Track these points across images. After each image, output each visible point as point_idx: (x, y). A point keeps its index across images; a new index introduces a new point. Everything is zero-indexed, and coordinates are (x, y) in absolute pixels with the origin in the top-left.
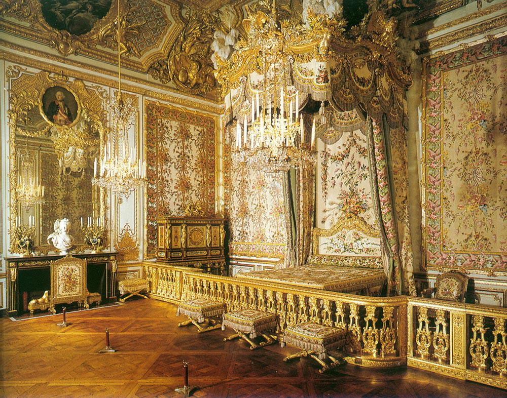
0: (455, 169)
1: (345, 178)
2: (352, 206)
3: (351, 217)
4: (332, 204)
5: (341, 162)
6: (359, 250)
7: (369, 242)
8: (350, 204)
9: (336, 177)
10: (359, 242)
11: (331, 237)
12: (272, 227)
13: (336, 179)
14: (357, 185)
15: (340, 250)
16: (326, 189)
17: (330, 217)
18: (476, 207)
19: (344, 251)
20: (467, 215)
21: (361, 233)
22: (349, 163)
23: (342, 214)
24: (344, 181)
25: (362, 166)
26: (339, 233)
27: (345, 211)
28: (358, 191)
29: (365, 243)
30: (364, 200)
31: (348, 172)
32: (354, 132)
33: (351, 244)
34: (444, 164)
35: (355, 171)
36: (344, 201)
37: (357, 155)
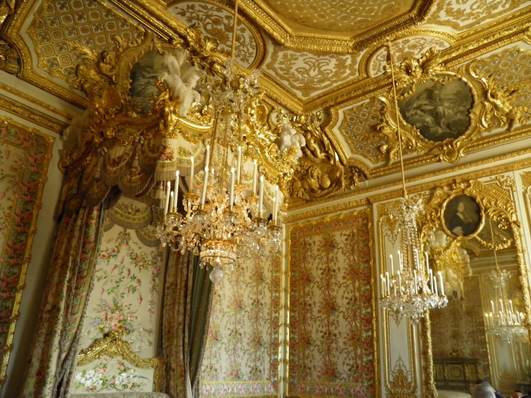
1: (109, 283)
5: (106, 261)
10: (124, 375)
13: (95, 282)
14: (123, 297)
22: (116, 266)
23: (97, 334)
24: (106, 288)
25: (132, 275)
26: (97, 361)
27: (102, 330)
28: (124, 306)
29: (131, 376)
30: (129, 319)
32: (128, 231)
35: (123, 278)
36: (102, 315)
37: (128, 260)
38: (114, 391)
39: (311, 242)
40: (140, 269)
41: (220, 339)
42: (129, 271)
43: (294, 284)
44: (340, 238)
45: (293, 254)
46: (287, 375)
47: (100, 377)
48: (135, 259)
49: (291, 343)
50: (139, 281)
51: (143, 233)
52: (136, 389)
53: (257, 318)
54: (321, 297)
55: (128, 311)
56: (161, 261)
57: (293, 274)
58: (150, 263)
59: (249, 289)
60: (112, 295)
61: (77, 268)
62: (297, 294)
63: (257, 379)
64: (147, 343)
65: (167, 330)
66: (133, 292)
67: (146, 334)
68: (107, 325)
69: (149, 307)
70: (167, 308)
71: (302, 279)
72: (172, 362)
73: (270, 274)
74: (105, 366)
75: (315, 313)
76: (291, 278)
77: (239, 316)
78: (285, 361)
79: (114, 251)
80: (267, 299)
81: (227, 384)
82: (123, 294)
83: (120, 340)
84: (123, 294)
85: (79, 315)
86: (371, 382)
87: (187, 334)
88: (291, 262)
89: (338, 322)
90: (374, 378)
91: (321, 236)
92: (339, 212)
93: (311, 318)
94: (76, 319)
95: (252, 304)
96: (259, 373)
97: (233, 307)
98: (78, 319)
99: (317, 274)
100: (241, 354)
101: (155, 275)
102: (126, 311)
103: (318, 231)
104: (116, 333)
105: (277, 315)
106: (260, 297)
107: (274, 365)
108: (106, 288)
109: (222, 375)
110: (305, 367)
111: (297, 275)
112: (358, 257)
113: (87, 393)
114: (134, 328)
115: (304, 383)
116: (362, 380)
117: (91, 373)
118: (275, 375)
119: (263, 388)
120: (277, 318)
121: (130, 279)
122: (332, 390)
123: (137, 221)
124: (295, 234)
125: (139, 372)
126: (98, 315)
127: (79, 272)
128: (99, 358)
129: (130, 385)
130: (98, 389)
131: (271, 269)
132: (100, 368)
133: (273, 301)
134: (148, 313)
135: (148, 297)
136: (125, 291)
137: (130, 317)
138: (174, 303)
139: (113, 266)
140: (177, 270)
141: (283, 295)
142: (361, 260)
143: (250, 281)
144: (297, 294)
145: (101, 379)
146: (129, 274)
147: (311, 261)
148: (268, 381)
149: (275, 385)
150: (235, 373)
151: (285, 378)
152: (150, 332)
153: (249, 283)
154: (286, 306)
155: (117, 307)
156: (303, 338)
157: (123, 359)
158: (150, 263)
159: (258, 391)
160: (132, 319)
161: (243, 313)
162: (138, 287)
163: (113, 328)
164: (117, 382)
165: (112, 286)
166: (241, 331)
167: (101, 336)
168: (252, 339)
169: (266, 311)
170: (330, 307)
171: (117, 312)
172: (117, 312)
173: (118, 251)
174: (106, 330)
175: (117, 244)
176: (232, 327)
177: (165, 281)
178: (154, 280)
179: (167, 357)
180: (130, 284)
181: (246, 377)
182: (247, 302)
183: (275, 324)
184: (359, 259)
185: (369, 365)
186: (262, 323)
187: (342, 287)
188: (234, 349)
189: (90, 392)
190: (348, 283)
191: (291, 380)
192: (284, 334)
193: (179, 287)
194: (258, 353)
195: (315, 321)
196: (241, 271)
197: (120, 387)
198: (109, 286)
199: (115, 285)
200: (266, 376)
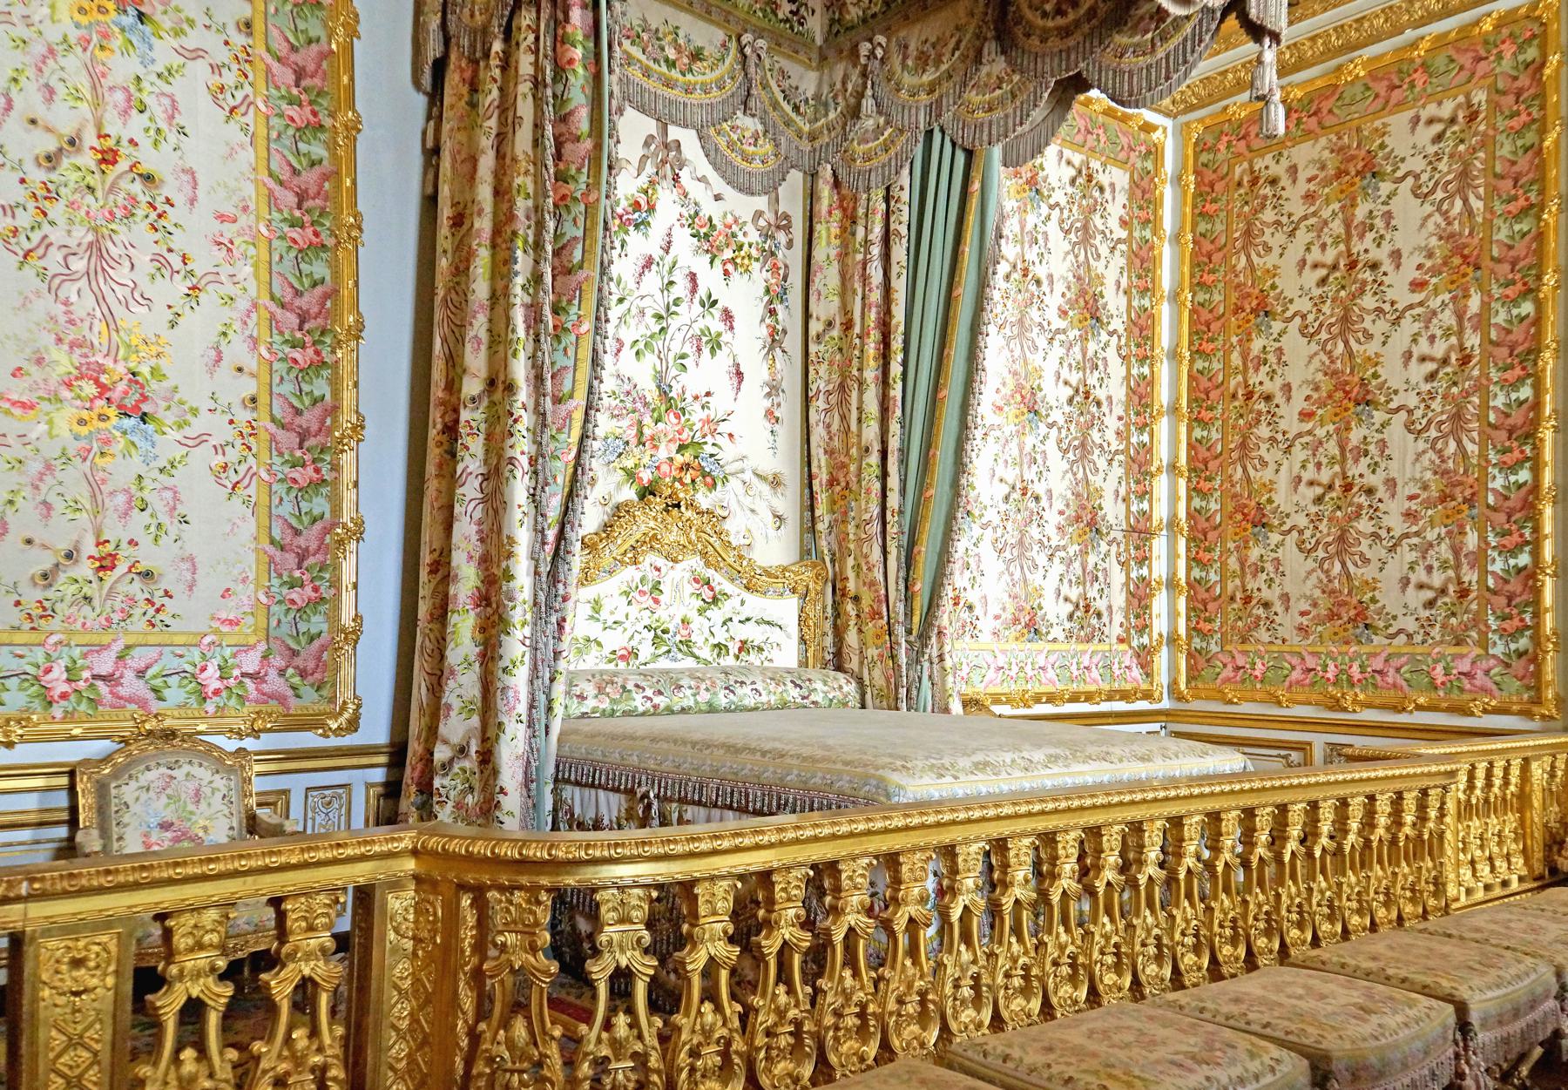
1: (632, 322)
2: (663, 454)
8: (655, 447)
10: (717, 615)
15: (633, 653)
21: (720, 582)
22: (649, 263)
23: (619, 486)
25: (702, 293)
26: (629, 574)
28: (688, 395)
29: (736, 620)
30: (709, 439)
32: (674, 133)
33: (685, 622)
35: (677, 302)
37: (684, 242)
38: (690, 663)
39: (1278, 170)
40: (726, 273)
41: (976, 512)
42: (693, 277)
43: (1202, 327)
44: (1406, 138)
45: (1203, 227)
46: (1182, 631)
48: (706, 236)
49: (1191, 528)
50: (727, 316)
51: (722, 142)
52: (753, 658)
53: (1084, 447)
54: (1316, 363)
55: (703, 415)
56: (790, 245)
57: (1201, 297)
58: (754, 253)
59: (1058, 351)
60: (650, 359)
61: (548, 237)
62: (1216, 366)
63: (1089, 640)
64: (770, 519)
65: (825, 477)
66: (713, 352)
67: (765, 488)
68: (646, 460)
69: (767, 403)
70: (820, 403)
71: (1238, 309)
72: (851, 574)
73: (1123, 300)
74: (656, 587)
75: (1290, 422)
76: (1193, 311)
77: (1030, 441)
78: (1172, 584)
79: (636, 206)
80: (1114, 387)
81: (1004, 652)
82: (683, 356)
83: (691, 505)
84: (683, 356)
85: (580, 399)
86: (1523, 643)
87: (894, 482)
88: (1194, 254)
89: (1383, 444)
90: (1537, 627)
91: (1323, 141)
92: (1410, 34)
93: (1273, 440)
94: (569, 415)
95: (1070, 401)
96: (1094, 621)
97: (1011, 411)
98: (578, 416)
99: (1296, 286)
100: (1042, 559)
101: (774, 297)
102: (697, 415)
103: (1312, 123)
104: (677, 485)
105: (1145, 438)
106: (1092, 380)
107: (1139, 597)
108: (627, 335)
109: (986, 625)
110: (1247, 600)
111: (1217, 297)
112: (1487, 200)
113: (611, 666)
114: (728, 469)
115: (1245, 653)
116: (1483, 635)
118: (1143, 629)
119: (1108, 667)
120: (1148, 449)
122: (1355, 669)
123: (697, 97)
124: (1213, 149)
125: (756, 605)
127: (556, 253)
129: (734, 648)
130: (642, 659)
131: (1124, 282)
132: (642, 593)
133: (1132, 391)
135: (757, 372)
138: (842, 388)
139: (641, 262)
140: (844, 277)
141: (1164, 371)
142: (1499, 208)
143: (1062, 324)
144: (1216, 366)
146: (694, 290)
147: (1276, 239)
148: (1124, 647)
149: (1144, 657)
150: (1025, 619)
151: (1173, 640)
152: (776, 482)
153: (1058, 331)
154: (1174, 409)
156: (1241, 508)
157: (708, 564)
158: (754, 253)
159: (1095, 674)
161: (1043, 429)
162: (726, 337)
164: (693, 638)
166: (1040, 489)
167: (629, 494)
168: (1070, 512)
169: (1112, 423)
170: (1353, 394)
173: (652, 209)
174: (646, 476)
175: (643, 181)
176: (1011, 475)
177: (807, 316)
178: (773, 312)
179: (833, 561)
180: (701, 324)
181: (1056, 632)
182: (1055, 394)
183: (1140, 466)
184: (1489, 209)
185: (1515, 585)
186: (1102, 463)
187: (1406, 322)
188: (1021, 542)
189: (622, 665)
190: (1435, 303)
191: (1197, 643)
192: (1167, 498)
193: (857, 330)
194: (1092, 559)
195: (1288, 451)
196: (1033, 288)
197: (706, 653)
199: (657, 329)
200: (1117, 631)
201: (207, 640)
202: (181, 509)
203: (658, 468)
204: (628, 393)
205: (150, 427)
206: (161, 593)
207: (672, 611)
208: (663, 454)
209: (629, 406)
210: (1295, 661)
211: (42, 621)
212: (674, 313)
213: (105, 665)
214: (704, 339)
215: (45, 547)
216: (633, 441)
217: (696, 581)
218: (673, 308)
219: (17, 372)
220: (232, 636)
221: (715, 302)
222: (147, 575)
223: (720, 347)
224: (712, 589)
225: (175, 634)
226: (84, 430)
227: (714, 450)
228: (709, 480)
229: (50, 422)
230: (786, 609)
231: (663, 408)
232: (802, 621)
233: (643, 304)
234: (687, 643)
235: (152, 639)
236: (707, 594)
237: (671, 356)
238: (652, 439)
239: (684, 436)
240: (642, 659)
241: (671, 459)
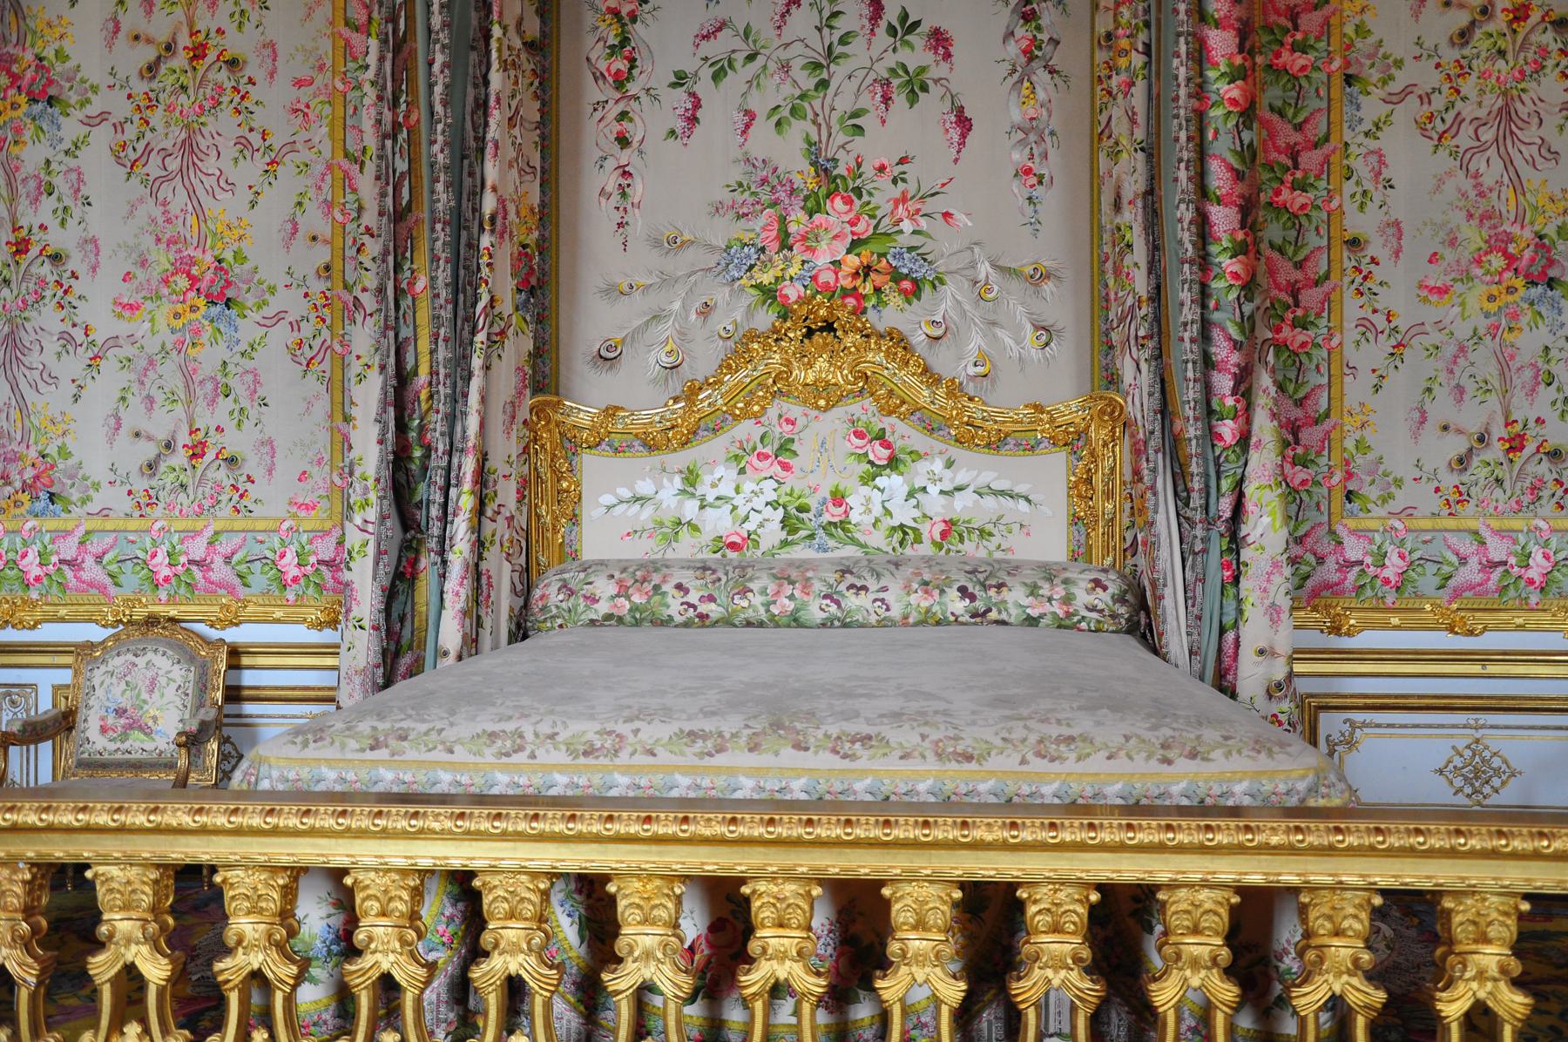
0: (1406, 92)
1: (770, 83)
2: (822, 260)
3: (829, 327)
4: (675, 244)
6: (894, 529)
7: (959, 481)
8: (813, 250)
9: (706, 73)
10: (893, 482)
11: (679, 459)
12: (135, 401)
13: (704, 87)
14: (859, 129)
16: (623, 141)
17: (667, 329)
18: (1511, 290)
19: (785, 543)
20: (1463, 331)
23: (750, 312)
24: (760, 103)
25: (891, 15)
26: (746, 430)
27: (769, 294)
28: (868, 170)
29: (933, 490)
30: (907, 226)
31: (798, 48)
34: (1347, 64)
35: (843, 40)
36: (760, 226)
38: (850, 551)
47: (772, 496)
50: (939, 40)
55: (896, 192)
60: (799, 130)
64: (1029, 327)
66: (913, 98)
67: (1015, 285)
68: (794, 270)
69: (1016, 156)
74: (785, 447)
102: (883, 194)
108: (760, 103)
114: (941, 265)
117: (720, 478)
121: (882, 38)
125: (977, 469)
126: (740, 230)
128: (746, 414)
130: (765, 544)
132: (762, 457)
134: (1016, 186)
136: (865, 101)
137: (911, 217)
145: (773, 505)
155: (831, 181)
160: (923, 223)
163: (827, 277)
164: (854, 517)
165: (788, 90)
167: (766, 318)
171: (838, 203)
172: (838, 203)
180: (891, 60)
198: (775, 92)
199: (808, 82)
201: (286, 525)
202: (261, 392)
203: (814, 278)
204: (764, 181)
205: (233, 312)
206: (244, 478)
207: (812, 480)
208: (822, 260)
209: (765, 198)
210: (1467, 546)
211: (148, 509)
212: (846, 56)
213: (198, 549)
214: (895, 82)
215: (149, 438)
216: (776, 245)
217: (859, 435)
218: (838, 50)
219: (127, 277)
220: (311, 522)
221: (917, 24)
222: (232, 461)
223: (924, 88)
224: (888, 445)
225: (257, 519)
226: (178, 324)
227: (916, 241)
228: (906, 285)
229: (152, 320)
230: (1049, 475)
231: (823, 191)
232: (1082, 486)
233: (784, 55)
234: (843, 525)
235: (238, 525)
236: (880, 454)
237: (835, 116)
238: (804, 238)
239: (860, 227)
240: (765, 544)
241: (837, 264)
